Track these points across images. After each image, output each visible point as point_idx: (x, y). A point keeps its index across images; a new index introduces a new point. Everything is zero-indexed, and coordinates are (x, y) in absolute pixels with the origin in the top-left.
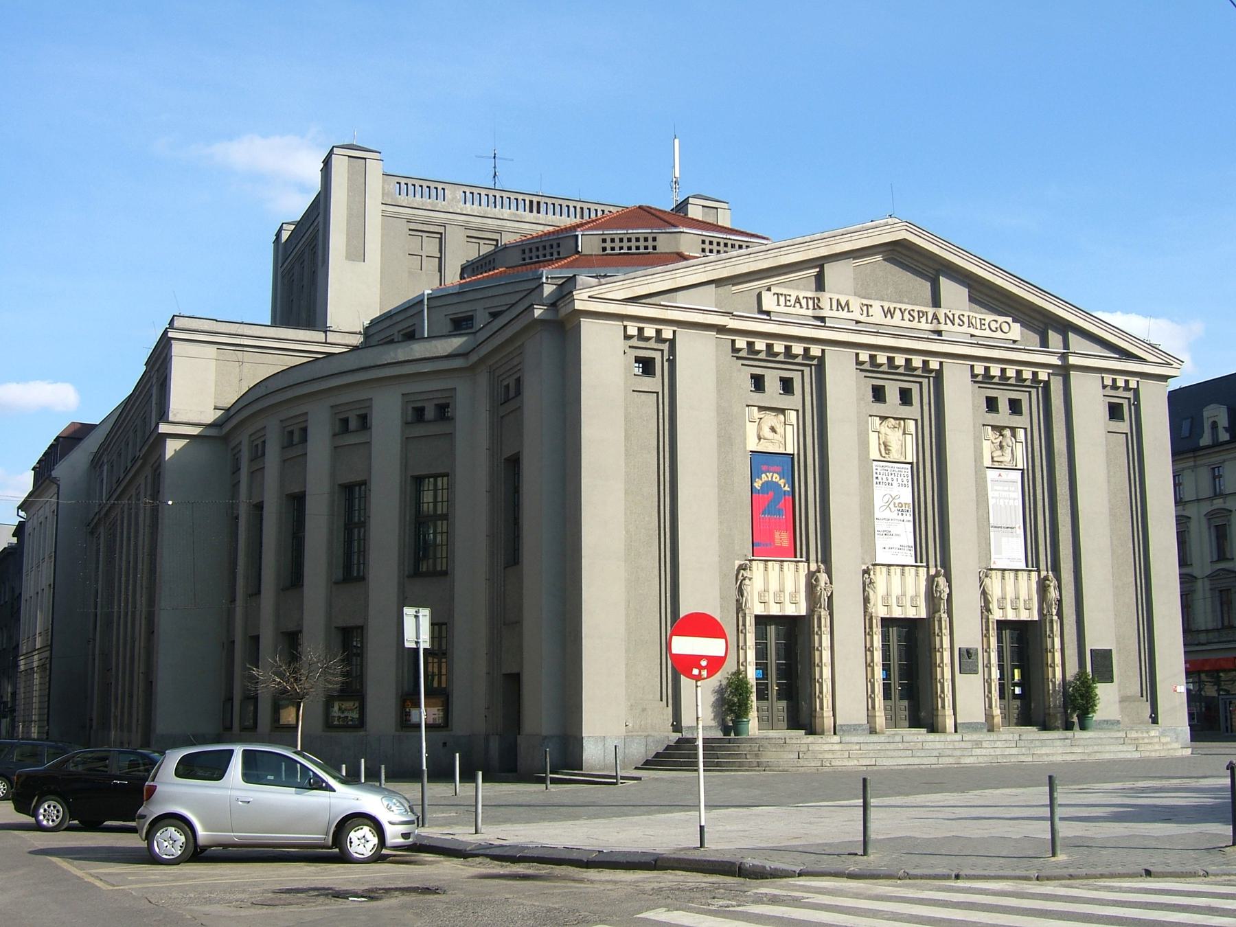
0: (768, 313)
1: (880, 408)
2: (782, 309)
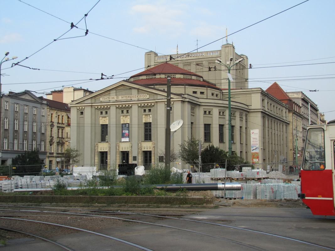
2: (104, 100)
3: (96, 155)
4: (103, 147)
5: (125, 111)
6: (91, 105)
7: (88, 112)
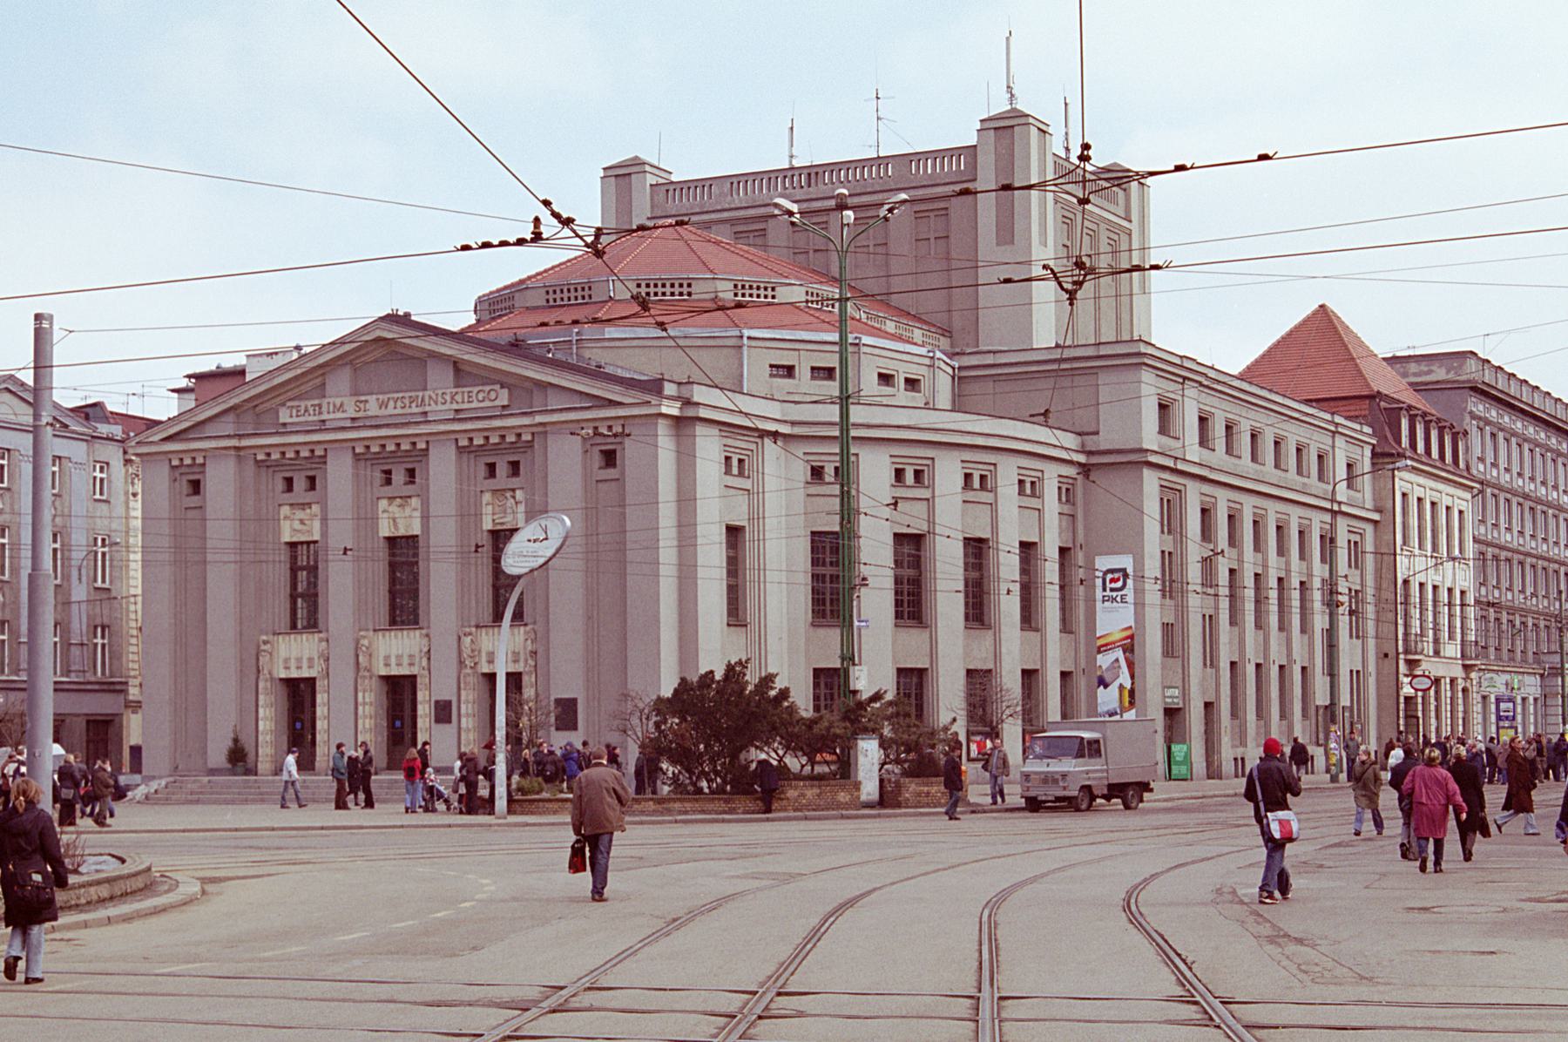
0: (284, 425)
1: (388, 491)
2: (295, 420)
3: (261, 697)
4: (295, 654)
5: (399, 477)
6: (234, 442)
7: (221, 480)
